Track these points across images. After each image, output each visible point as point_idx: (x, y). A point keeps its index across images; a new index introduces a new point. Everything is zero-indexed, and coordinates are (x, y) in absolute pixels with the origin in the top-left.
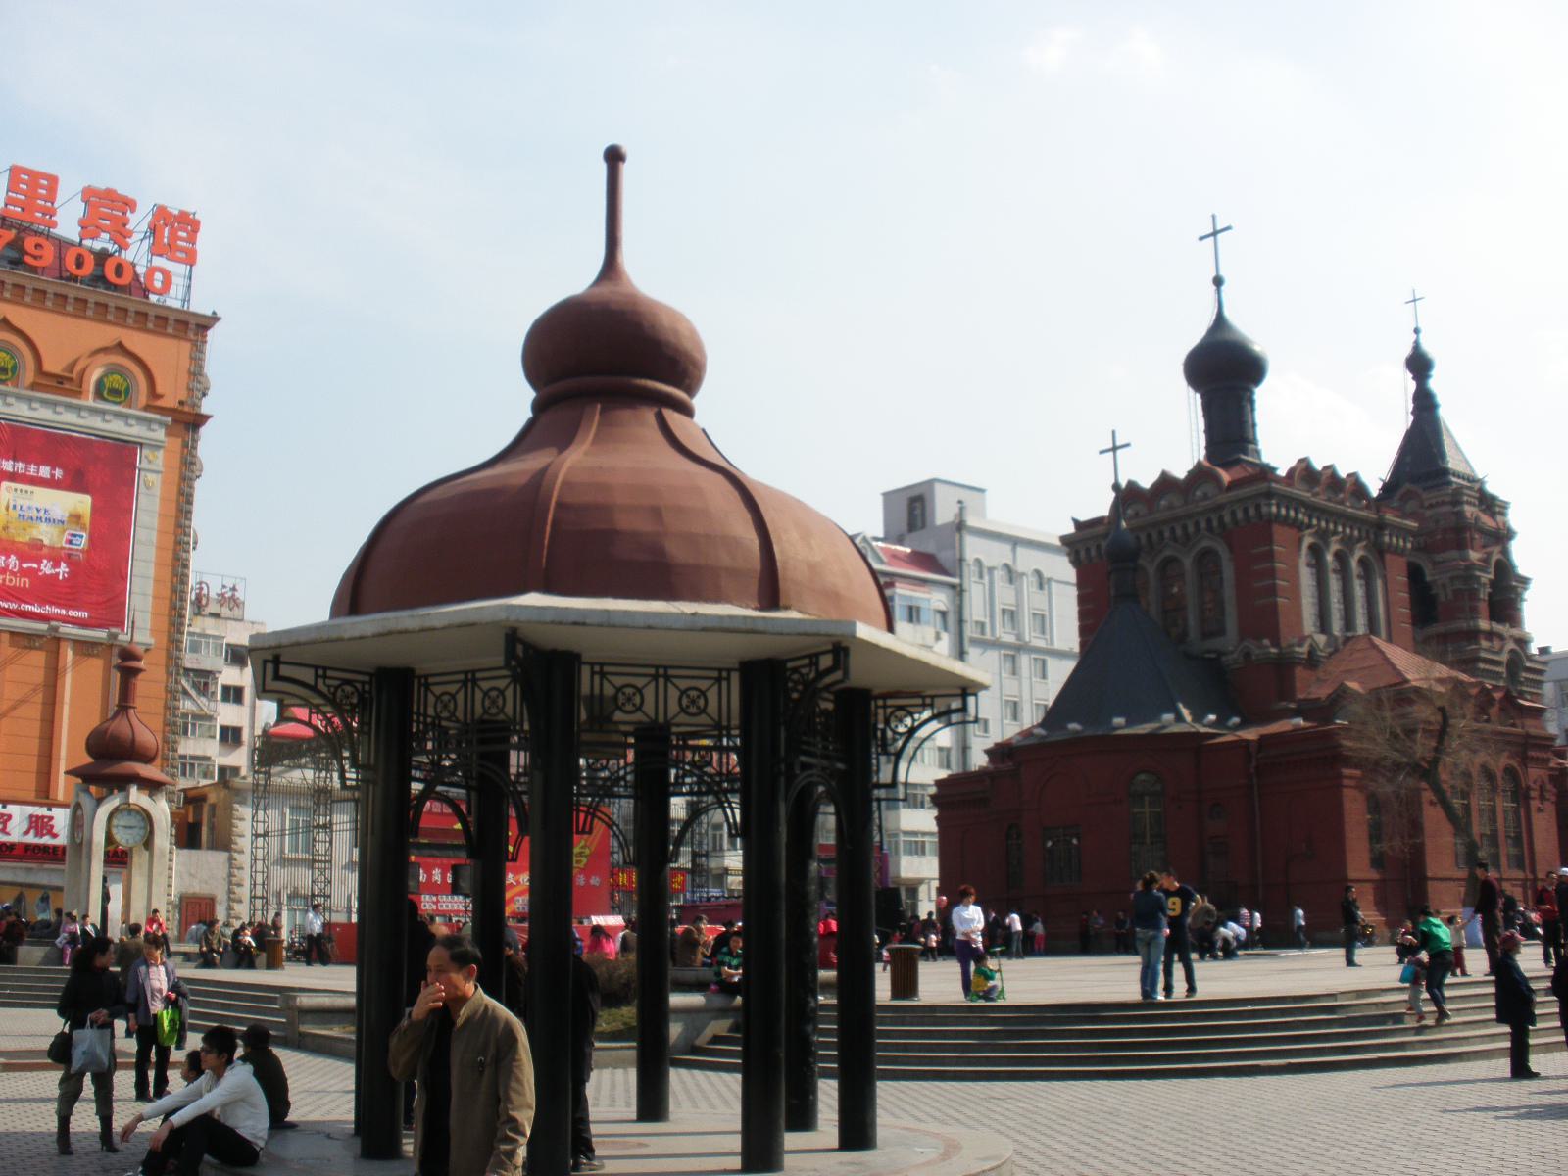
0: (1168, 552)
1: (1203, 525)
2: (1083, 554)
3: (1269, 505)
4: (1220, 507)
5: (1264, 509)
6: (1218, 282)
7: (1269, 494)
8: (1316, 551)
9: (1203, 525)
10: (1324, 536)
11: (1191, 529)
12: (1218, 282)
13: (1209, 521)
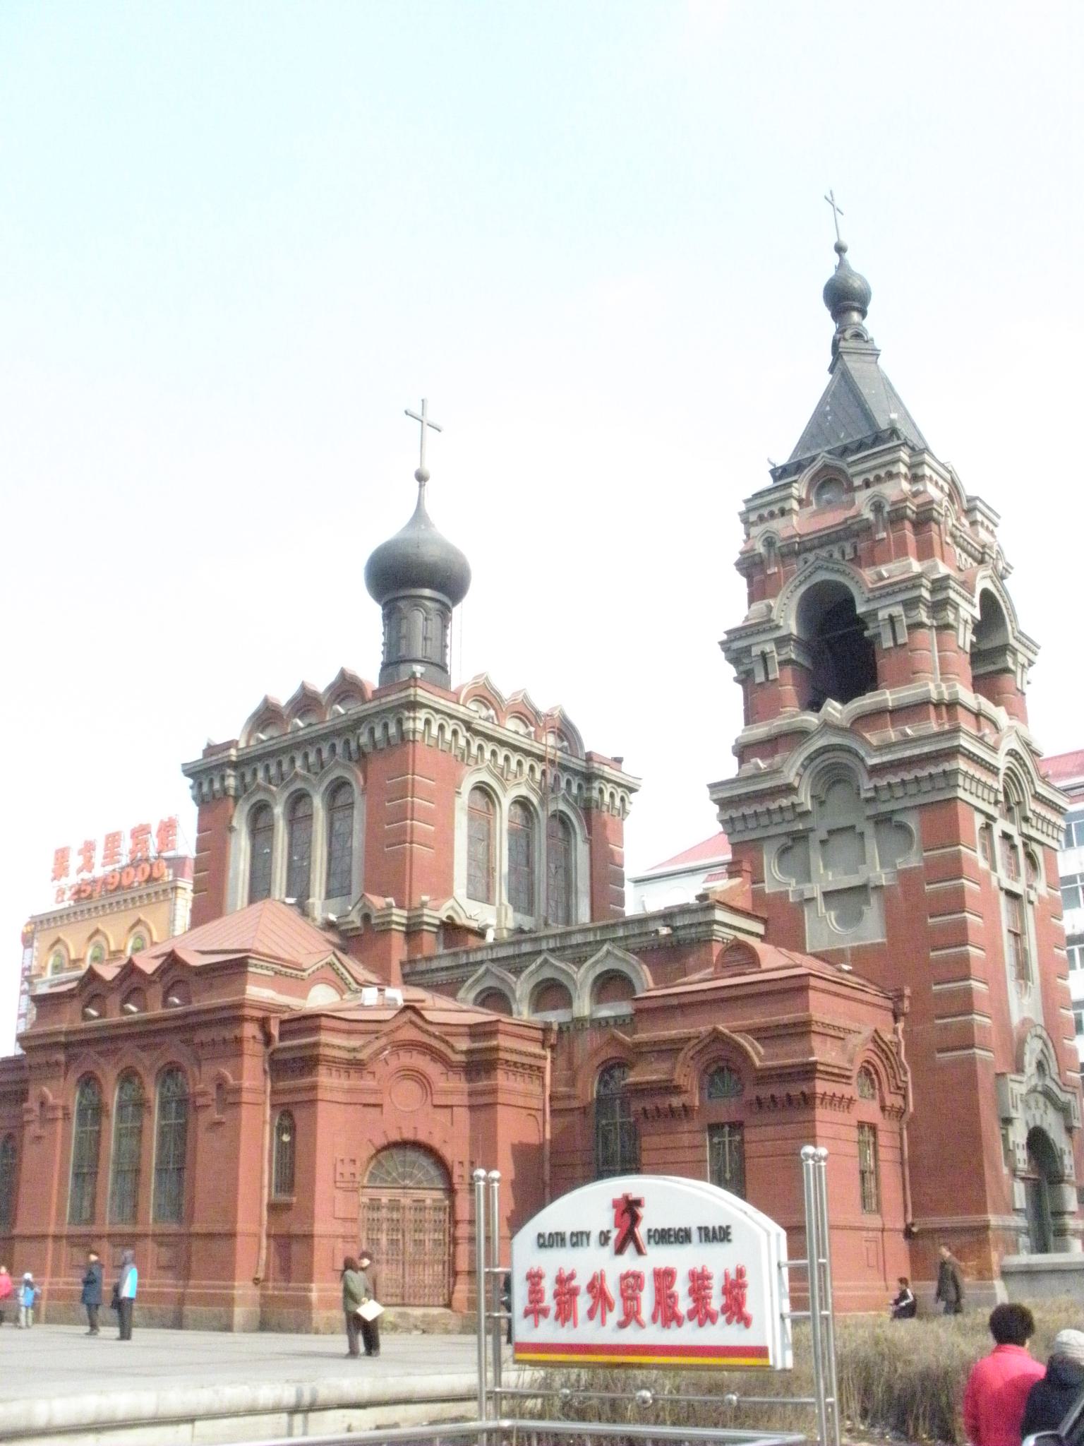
0: (298, 785)
1: (339, 749)
2: (205, 788)
3: (414, 719)
4: (358, 722)
5: (409, 725)
7: (414, 705)
8: (482, 789)
9: (339, 749)
10: (501, 776)
11: (325, 754)
12: (421, 478)
13: (347, 742)
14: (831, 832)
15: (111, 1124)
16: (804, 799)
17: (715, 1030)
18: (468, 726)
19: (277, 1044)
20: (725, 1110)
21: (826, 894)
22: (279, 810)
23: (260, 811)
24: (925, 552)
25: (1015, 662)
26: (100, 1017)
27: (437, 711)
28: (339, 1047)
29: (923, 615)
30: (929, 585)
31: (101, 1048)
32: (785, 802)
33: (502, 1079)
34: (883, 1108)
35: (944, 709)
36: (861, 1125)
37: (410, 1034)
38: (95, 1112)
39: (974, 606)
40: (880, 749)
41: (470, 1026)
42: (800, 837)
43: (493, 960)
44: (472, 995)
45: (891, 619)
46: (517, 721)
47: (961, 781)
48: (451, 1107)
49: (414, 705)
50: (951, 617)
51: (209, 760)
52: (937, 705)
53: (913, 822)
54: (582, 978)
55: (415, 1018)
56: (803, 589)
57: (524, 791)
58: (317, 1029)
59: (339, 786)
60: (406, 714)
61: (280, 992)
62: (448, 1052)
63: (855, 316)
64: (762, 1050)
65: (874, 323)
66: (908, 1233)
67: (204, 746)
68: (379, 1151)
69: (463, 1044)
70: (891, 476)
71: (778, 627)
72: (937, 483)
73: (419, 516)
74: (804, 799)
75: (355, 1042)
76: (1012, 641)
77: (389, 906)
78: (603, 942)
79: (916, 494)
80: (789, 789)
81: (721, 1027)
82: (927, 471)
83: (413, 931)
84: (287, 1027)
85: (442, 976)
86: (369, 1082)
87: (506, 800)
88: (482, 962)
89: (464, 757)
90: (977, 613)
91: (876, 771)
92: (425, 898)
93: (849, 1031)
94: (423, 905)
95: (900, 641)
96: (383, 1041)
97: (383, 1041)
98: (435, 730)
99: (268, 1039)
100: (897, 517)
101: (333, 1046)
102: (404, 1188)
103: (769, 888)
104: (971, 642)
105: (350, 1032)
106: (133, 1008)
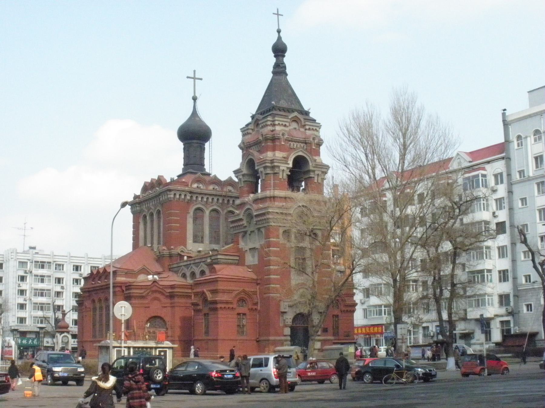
6: (195, 99)
7: (170, 190)
12: (195, 99)
14: (251, 232)
15: (98, 312)
16: (245, 222)
17: (203, 291)
18: (191, 192)
19: (125, 292)
20: (206, 310)
21: (250, 249)
22: (155, 214)
23: (145, 217)
24: (274, 149)
25: (314, 174)
26: (95, 284)
27: (178, 191)
28: (137, 293)
29: (269, 171)
30: (269, 162)
31: (94, 292)
32: (241, 223)
33: (176, 300)
34: (249, 309)
35: (272, 199)
36: (239, 314)
37: (154, 288)
38: (95, 309)
39: (289, 164)
40: (257, 210)
41: (170, 286)
42: (245, 232)
43: (184, 265)
44: (181, 275)
45: (261, 172)
46: (214, 185)
47: (271, 220)
48: (166, 307)
49: (170, 190)
50: (277, 170)
51: (147, 193)
52: (270, 197)
53: (263, 230)
54: (197, 271)
55: (156, 284)
56: (247, 160)
57: (215, 207)
58: (131, 289)
59: (159, 212)
60: (168, 193)
61: (127, 278)
62: (164, 293)
63: (280, 58)
64: (211, 296)
65: (287, 60)
66: (257, 341)
67: (133, 196)
68: (151, 318)
69: (169, 290)
70: (267, 125)
71: (242, 171)
72: (282, 124)
73: (195, 113)
74: (245, 222)
75: (142, 291)
76: (311, 168)
77: (164, 250)
78: (200, 262)
79: (272, 131)
80: (241, 220)
81: (205, 290)
82: (277, 123)
83: (171, 256)
84: (127, 288)
85: (176, 269)
86: (146, 301)
87: (207, 212)
88: (182, 266)
89: (189, 202)
90: (291, 165)
91: (257, 216)
92: (172, 247)
93: (234, 290)
94: (172, 249)
95: (264, 178)
96: (148, 291)
97: (148, 291)
98: (178, 196)
99: (123, 291)
100: (266, 139)
101: (134, 293)
102: (156, 328)
103: (240, 247)
104: (288, 175)
105: (142, 289)
106: (100, 282)
